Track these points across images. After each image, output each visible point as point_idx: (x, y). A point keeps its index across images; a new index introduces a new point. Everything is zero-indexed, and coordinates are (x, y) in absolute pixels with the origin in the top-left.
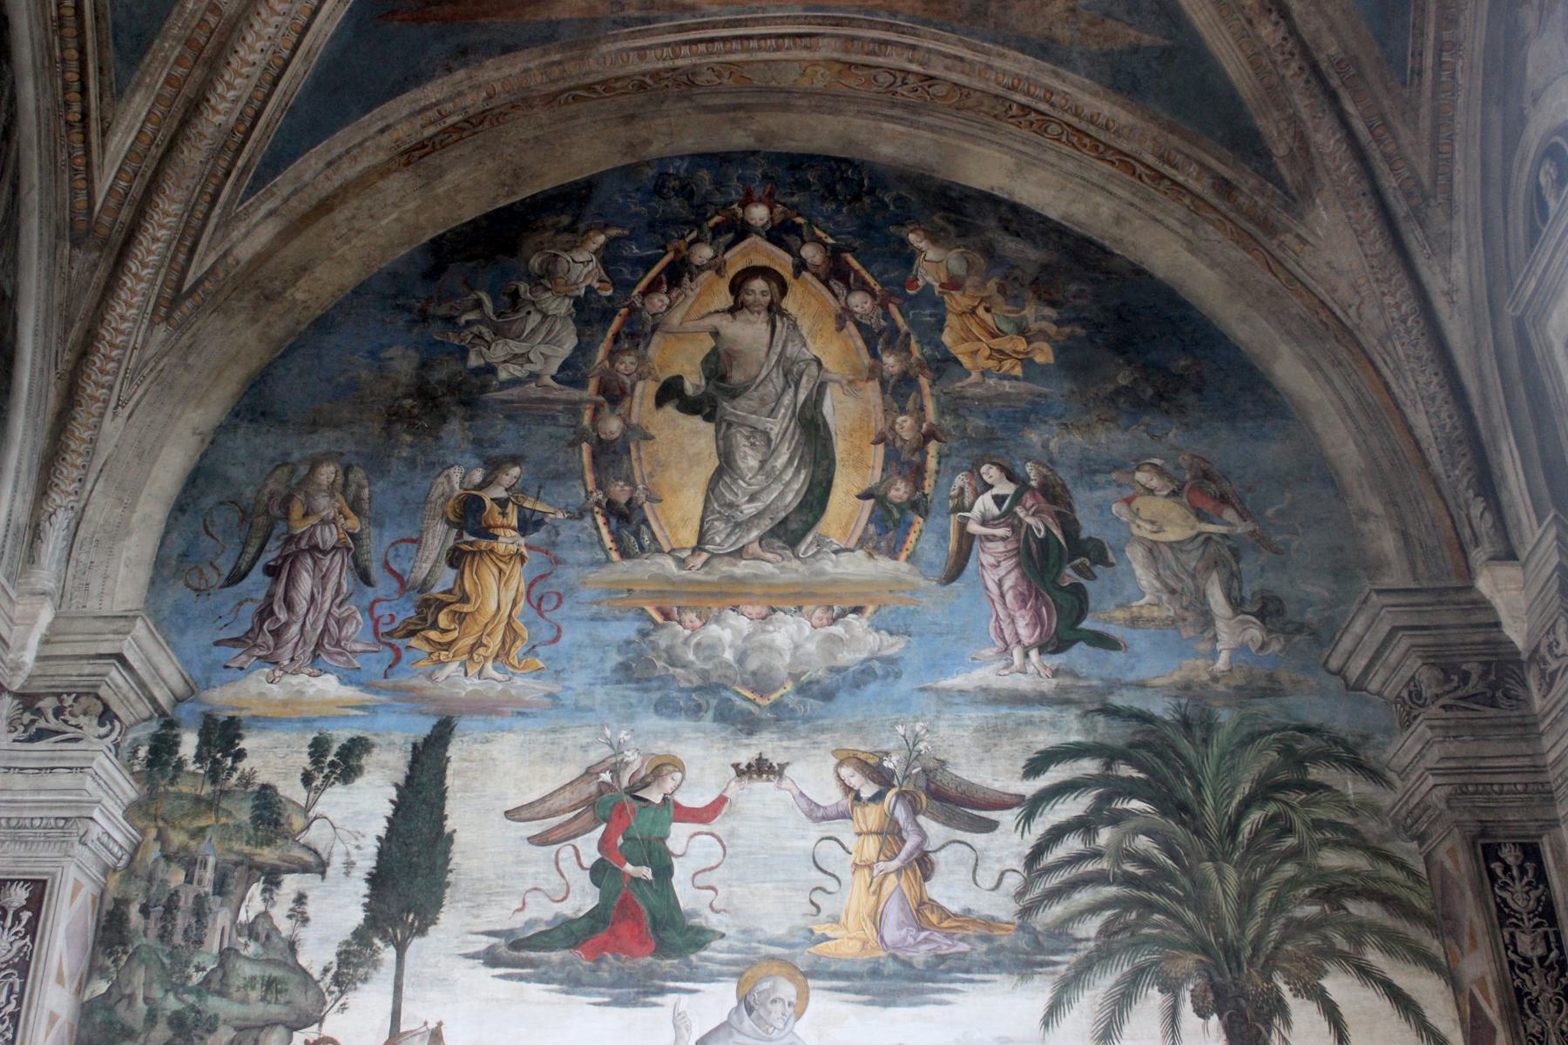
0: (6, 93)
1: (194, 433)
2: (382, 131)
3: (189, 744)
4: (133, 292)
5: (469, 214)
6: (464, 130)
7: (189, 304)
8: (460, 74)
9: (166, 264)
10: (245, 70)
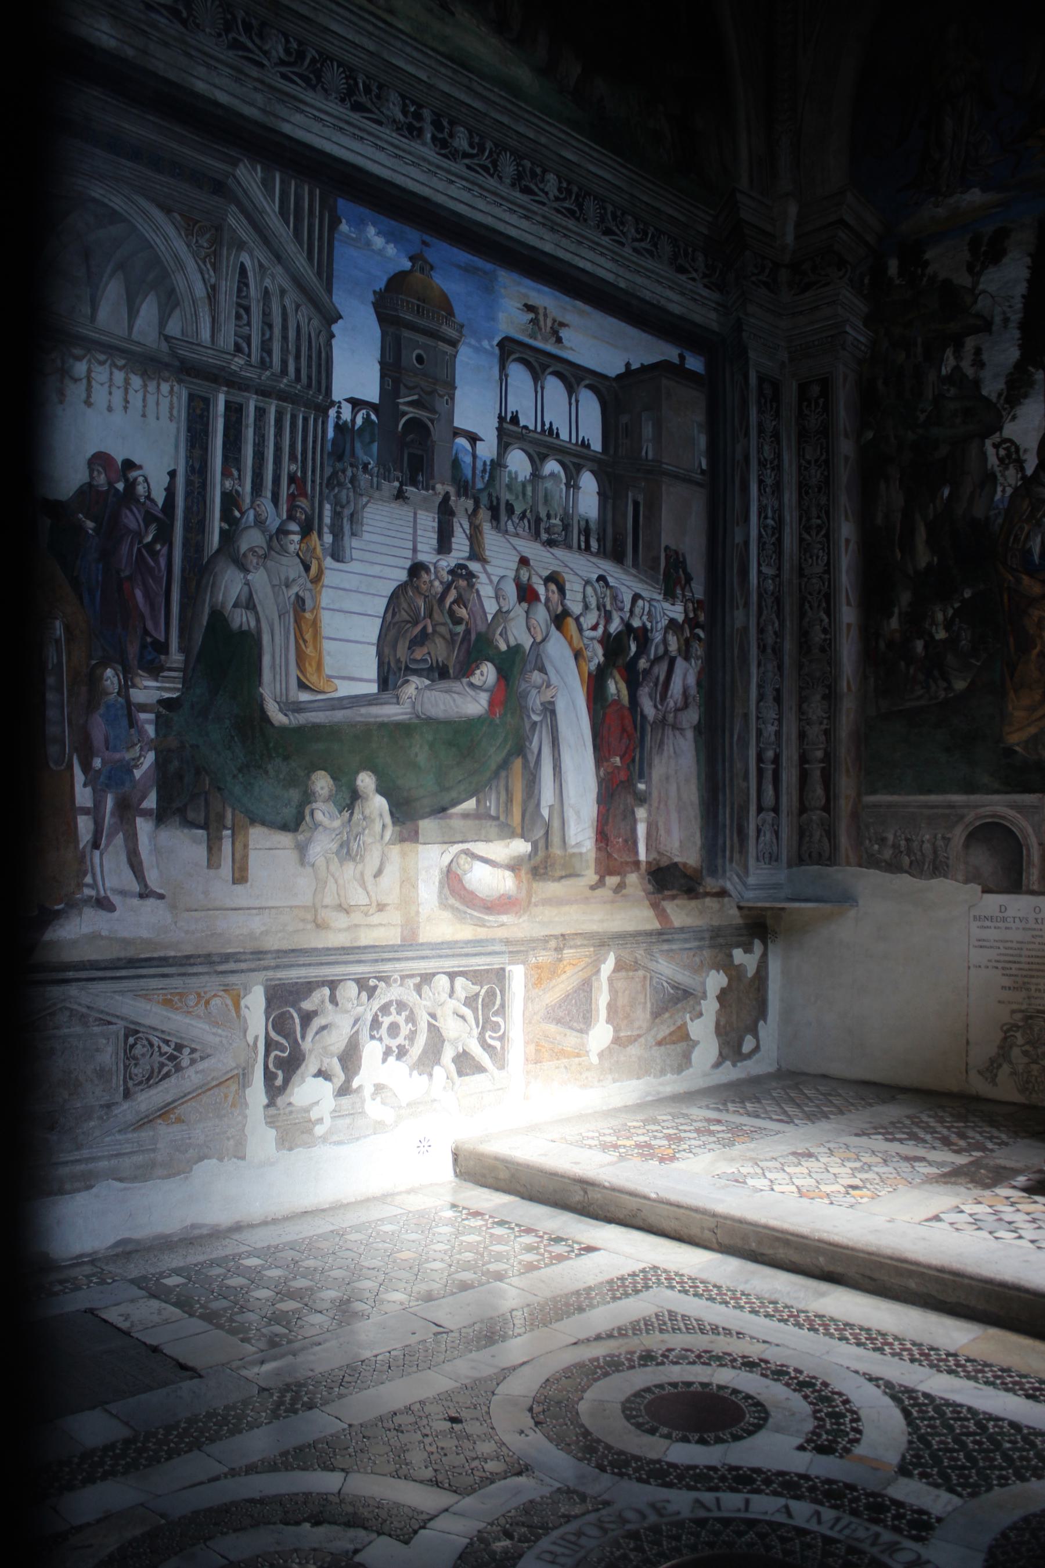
3: (893, 267)
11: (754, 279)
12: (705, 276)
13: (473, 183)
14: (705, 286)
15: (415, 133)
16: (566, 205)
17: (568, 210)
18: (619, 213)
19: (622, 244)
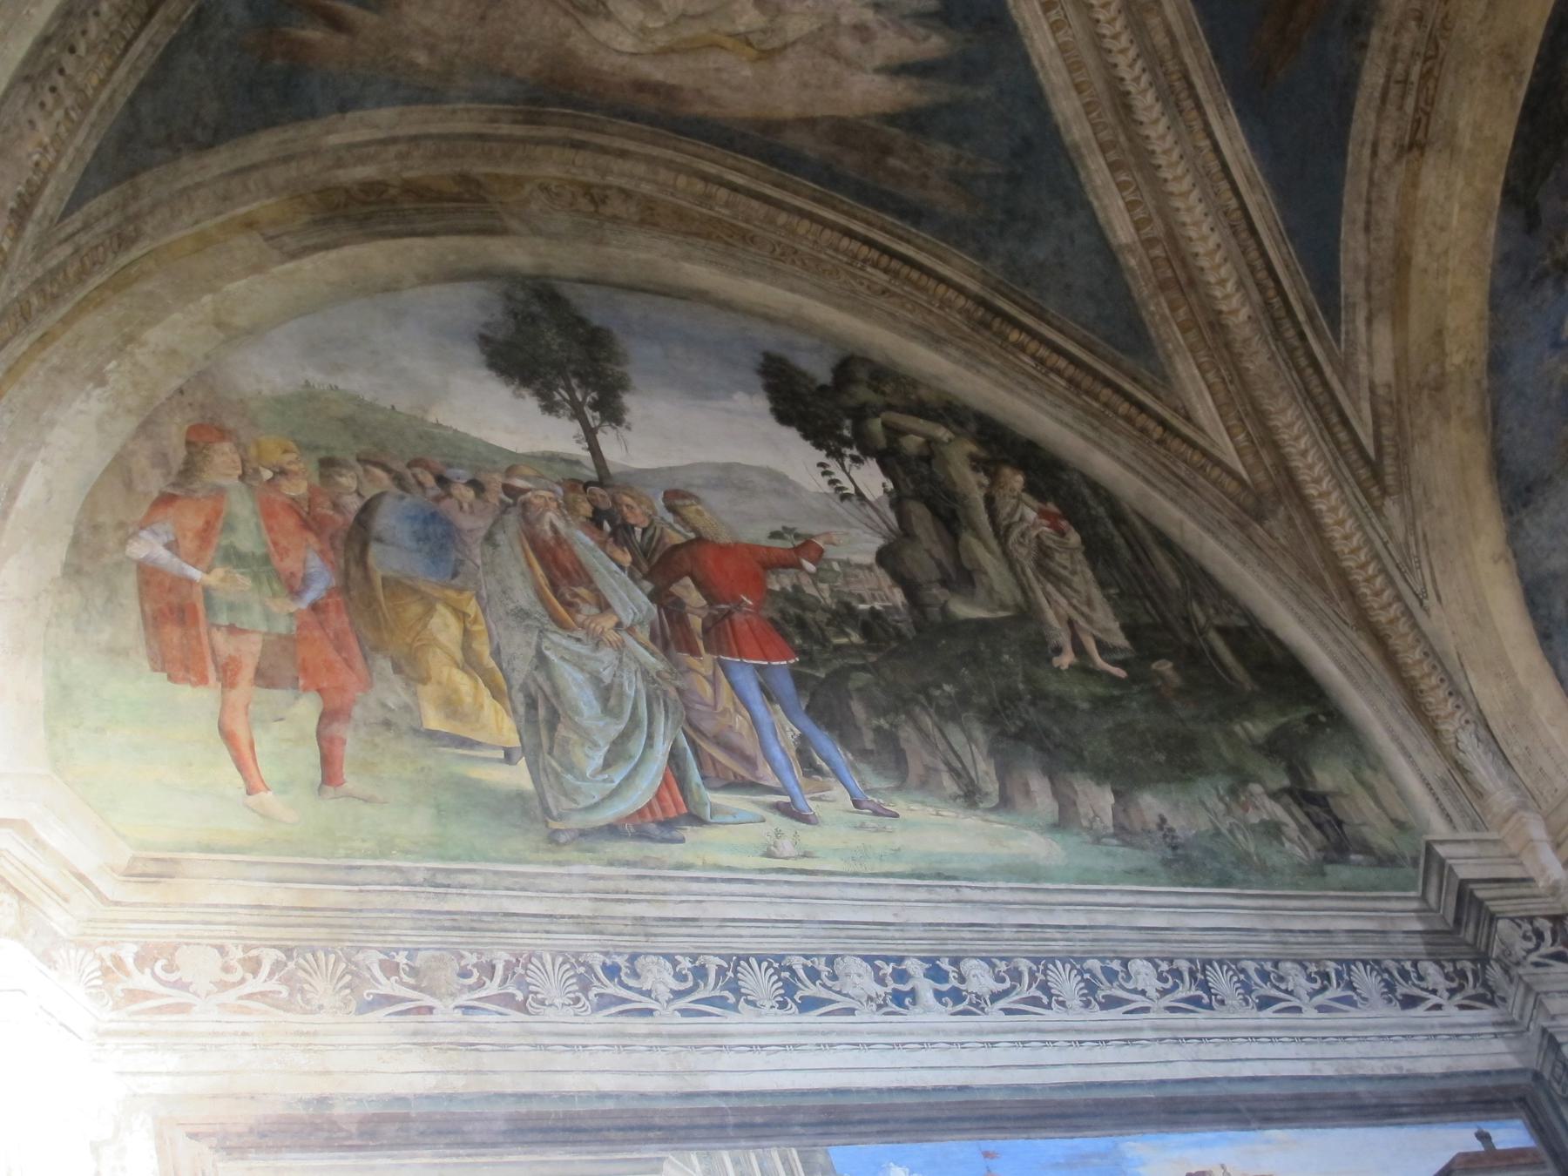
0: (1086, 492)
1: (1496, 562)
2: (1374, 154)
4: (1333, 510)
5: (1505, 133)
6: (1430, 71)
7: (1389, 466)
8: (1375, 37)
9: (1338, 455)
10: (1218, 258)
11: (1533, 957)
12: (1452, 992)
13: (1024, 1031)
14: (1462, 1007)
15: (907, 1001)
16: (1182, 993)
17: (1188, 1000)
18: (1268, 967)
19: (1298, 1009)
